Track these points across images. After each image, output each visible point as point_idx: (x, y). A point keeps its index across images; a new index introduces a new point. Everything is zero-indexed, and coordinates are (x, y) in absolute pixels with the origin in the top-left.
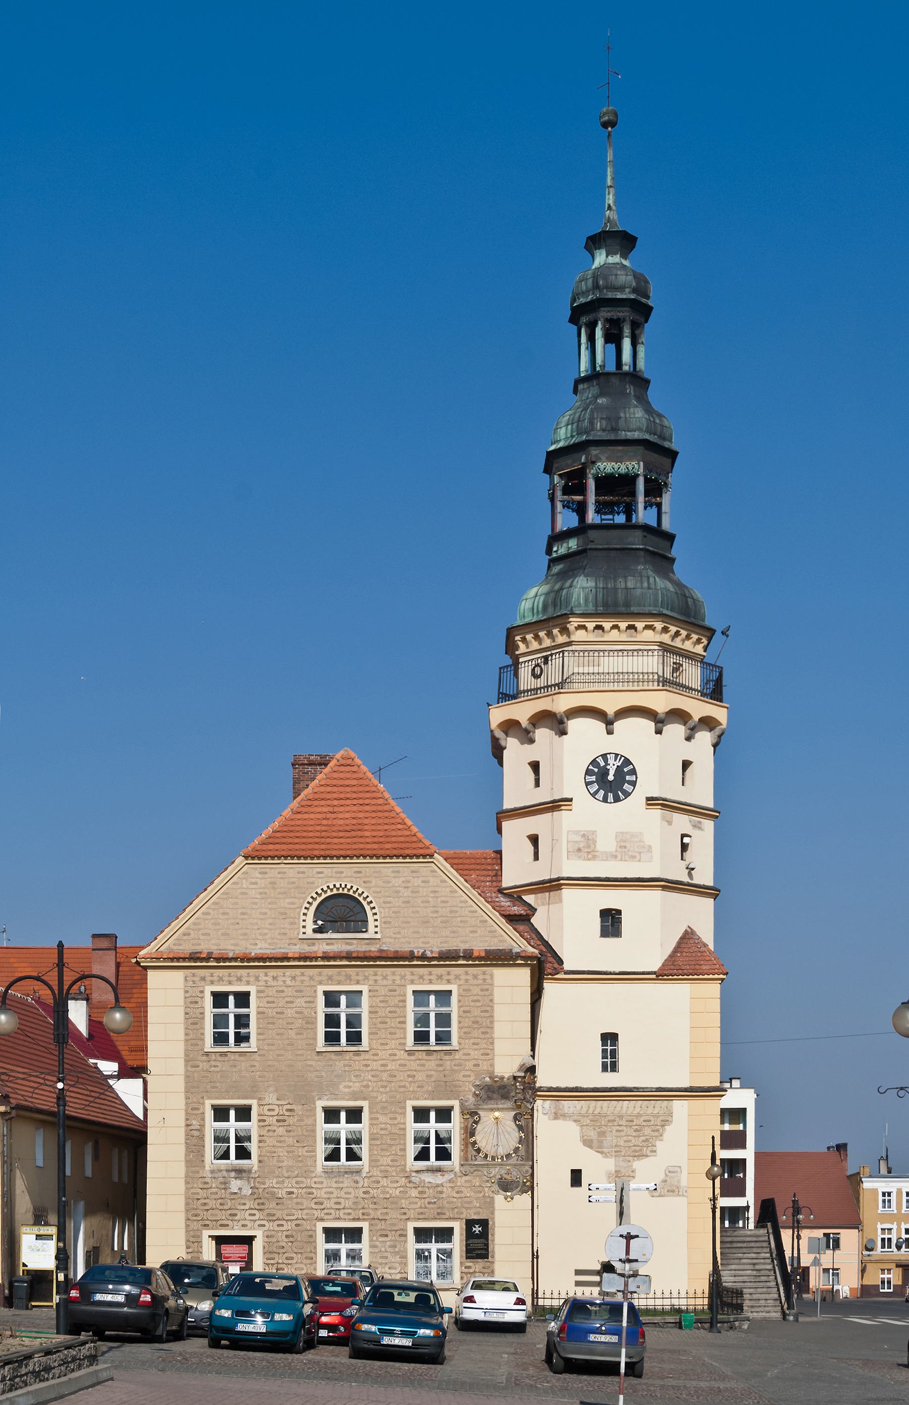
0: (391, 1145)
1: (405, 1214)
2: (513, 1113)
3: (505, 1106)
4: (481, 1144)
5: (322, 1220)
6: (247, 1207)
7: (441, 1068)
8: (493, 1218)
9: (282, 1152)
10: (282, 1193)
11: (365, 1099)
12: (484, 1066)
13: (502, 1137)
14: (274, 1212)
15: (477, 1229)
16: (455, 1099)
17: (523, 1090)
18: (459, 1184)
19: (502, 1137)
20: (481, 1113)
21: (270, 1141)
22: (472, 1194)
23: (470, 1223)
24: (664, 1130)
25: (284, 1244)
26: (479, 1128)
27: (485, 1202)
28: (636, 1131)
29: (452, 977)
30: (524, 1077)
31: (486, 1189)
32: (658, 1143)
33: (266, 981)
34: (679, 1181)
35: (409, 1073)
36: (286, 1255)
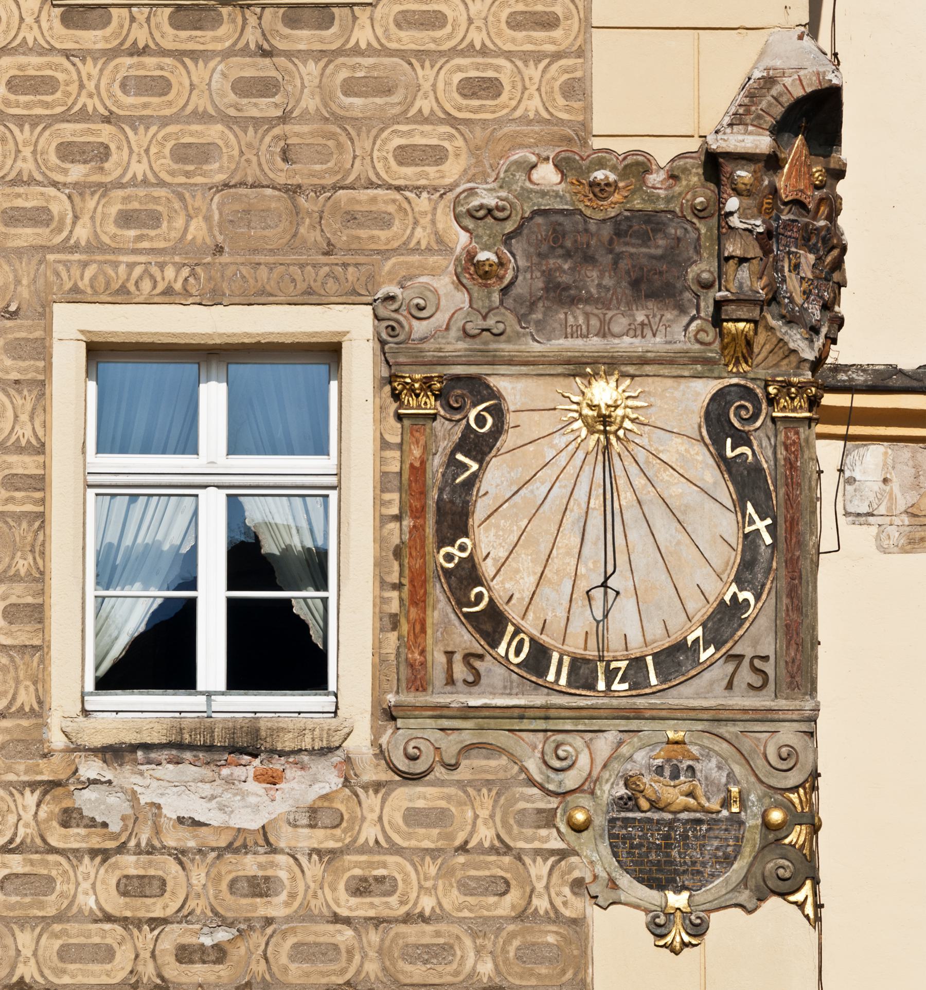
3: (655, 344)
4: (508, 583)
7: (265, 107)
13: (637, 534)
16: (351, 297)
17: (766, 239)
18: (370, 833)
19: (637, 534)
20: (512, 388)
22: (452, 899)
26: (496, 478)
27: (531, 953)
30: (772, 162)
31: (539, 869)
35: (70, 131)
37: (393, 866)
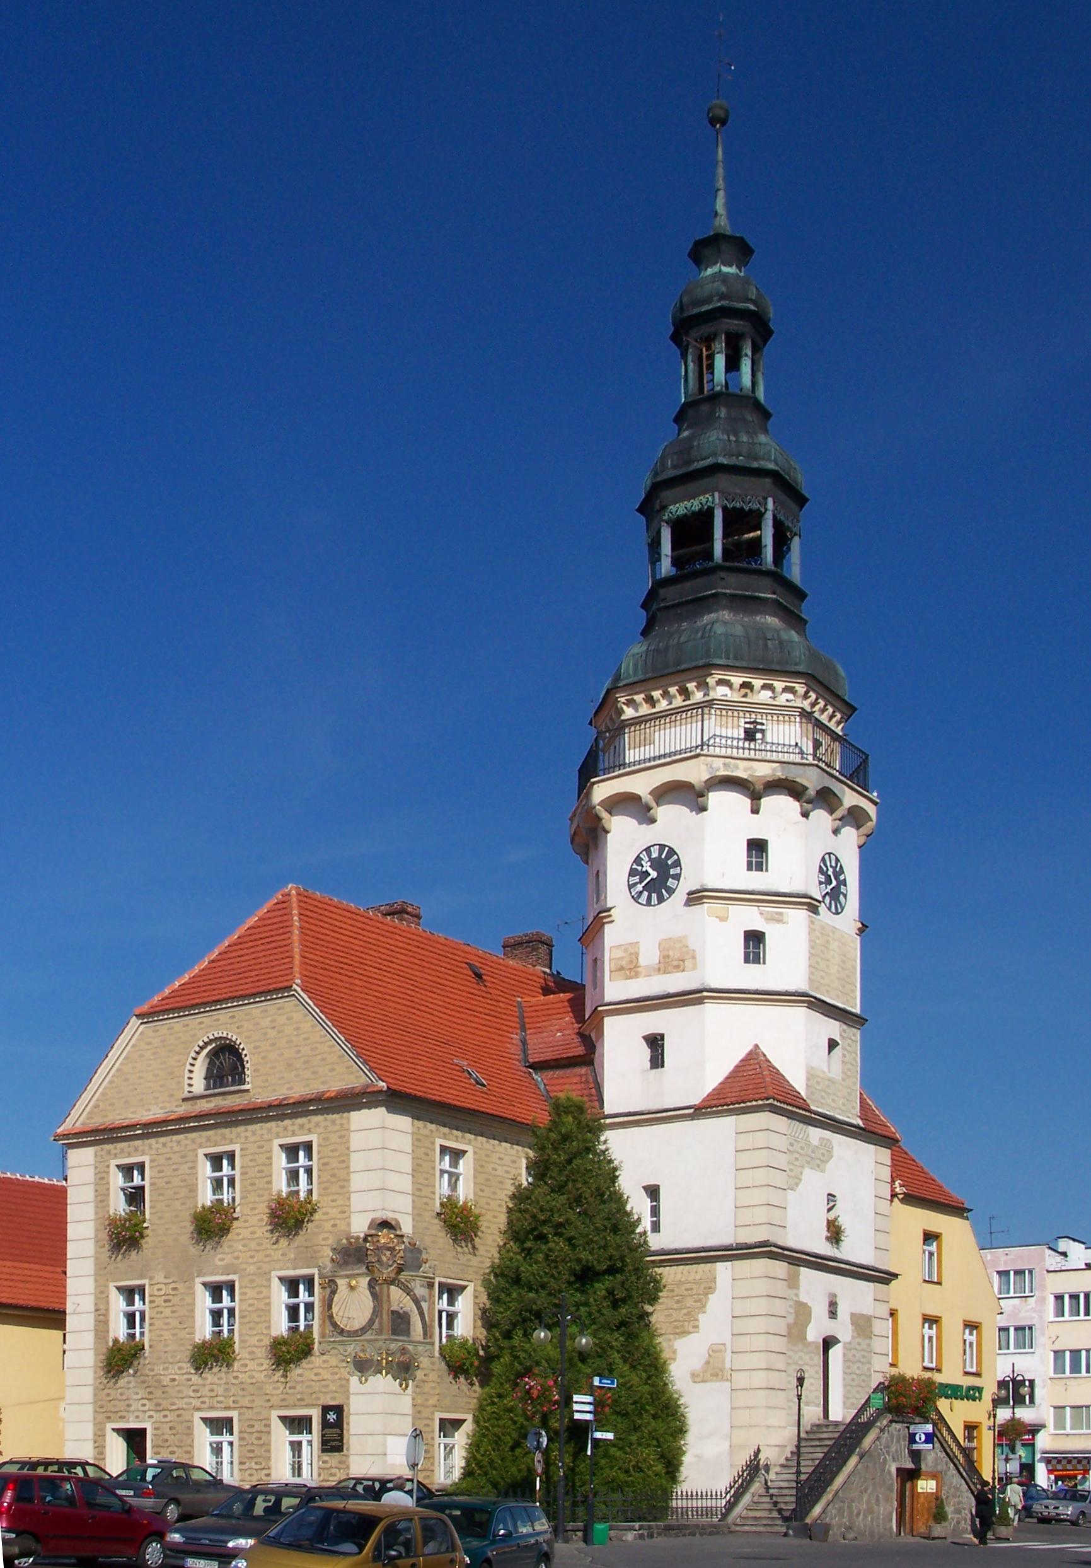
0: (258, 1323)
1: (269, 1400)
2: (368, 1279)
5: (198, 1409)
6: (139, 1397)
8: (348, 1405)
9: (167, 1335)
10: (166, 1381)
11: (235, 1273)
12: (342, 1226)
14: (160, 1401)
15: (332, 1417)
20: (339, 1281)
21: (159, 1324)
23: (326, 1409)
24: (707, 1299)
25: (167, 1437)
28: (678, 1302)
29: (312, 1125)
32: (701, 1316)
33: (157, 1149)
34: (723, 1362)
36: (170, 1449)
37: (321, 1371)
